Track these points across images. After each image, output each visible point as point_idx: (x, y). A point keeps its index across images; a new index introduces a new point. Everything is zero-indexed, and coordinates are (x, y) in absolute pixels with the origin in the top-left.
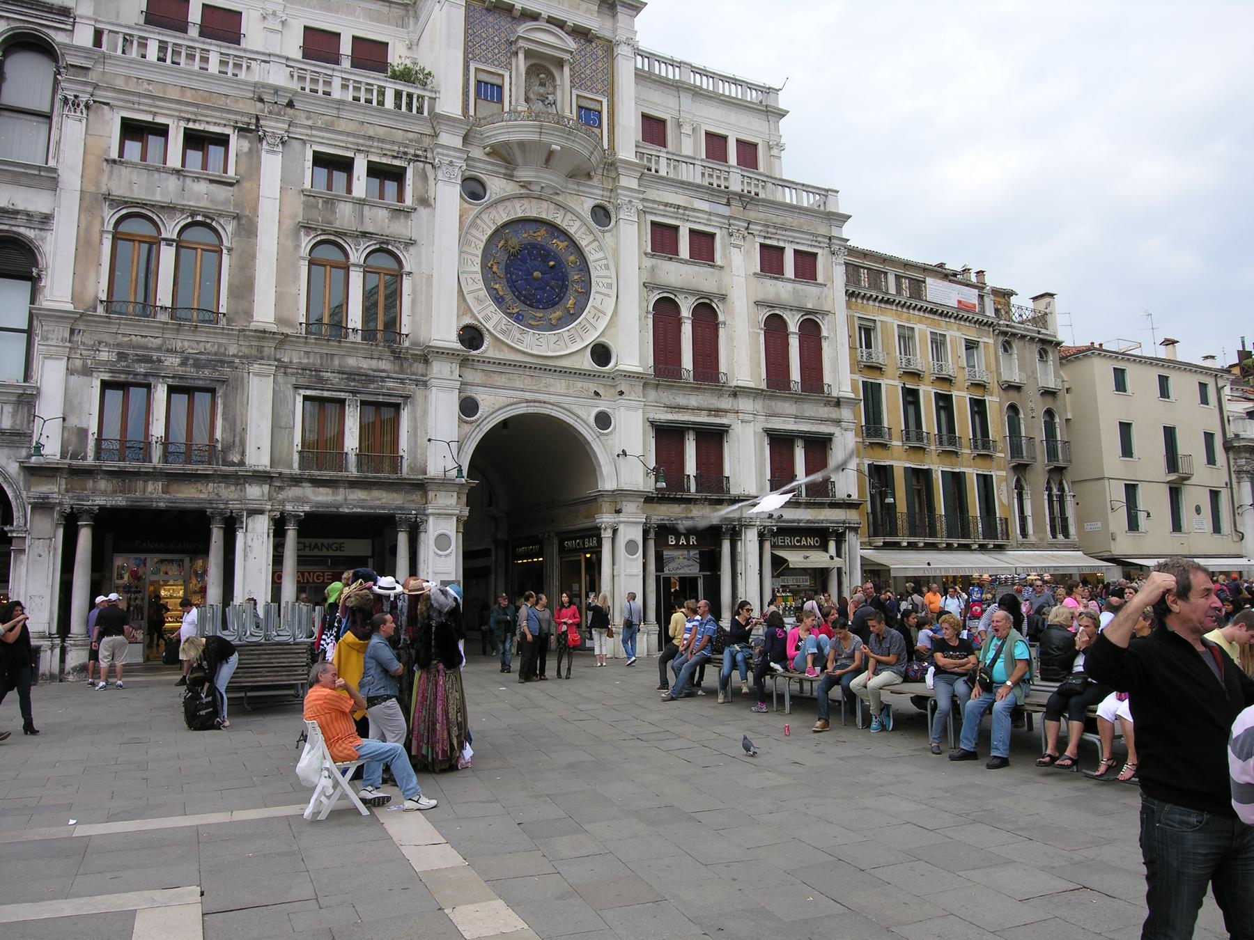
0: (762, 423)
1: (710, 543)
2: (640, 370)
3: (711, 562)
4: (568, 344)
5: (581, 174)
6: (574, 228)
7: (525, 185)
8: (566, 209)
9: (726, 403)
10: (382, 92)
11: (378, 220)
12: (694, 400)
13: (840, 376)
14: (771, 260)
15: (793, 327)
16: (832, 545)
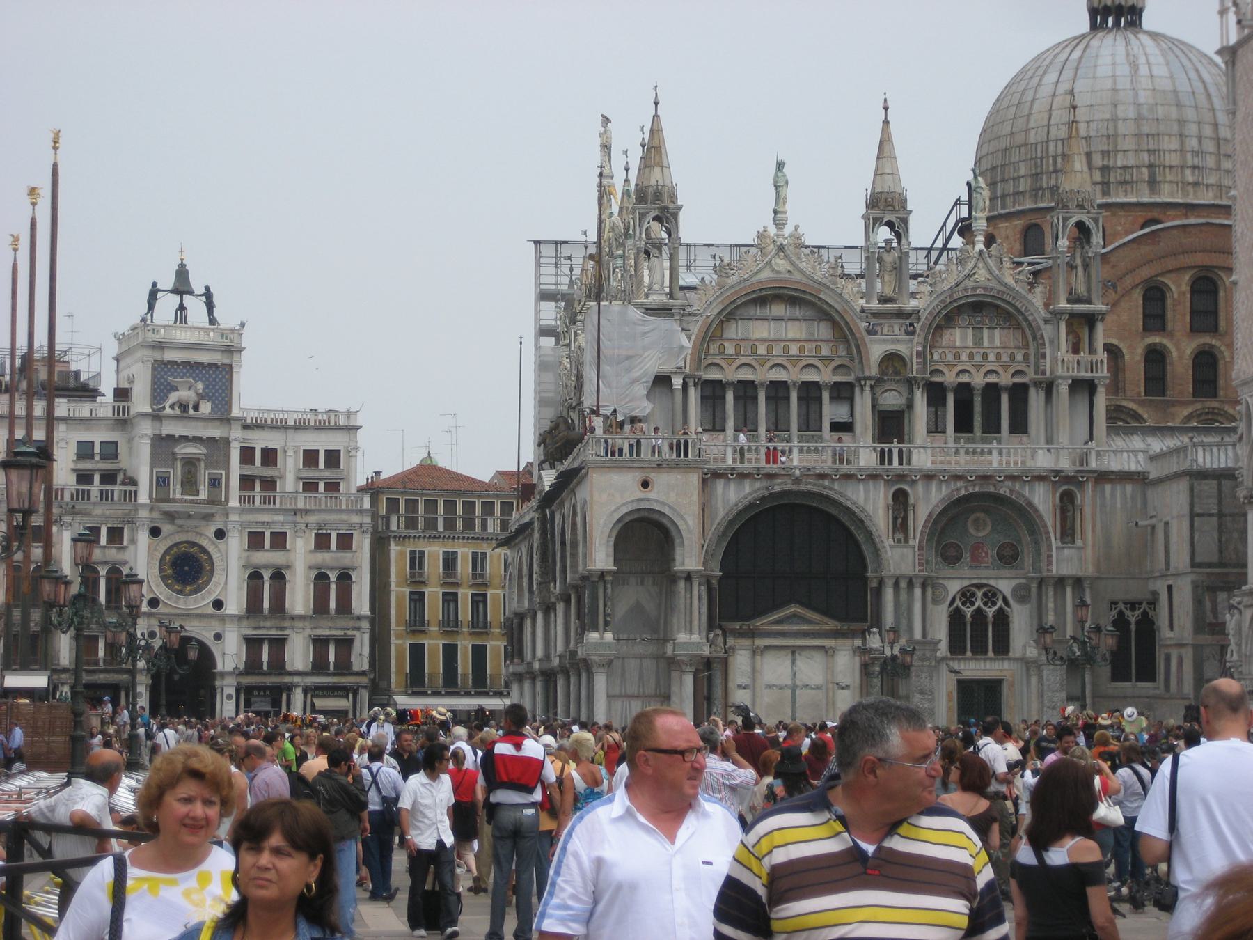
0: (308, 631)
1: (277, 694)
2: (236, 612)
3: (276, 703)
4: (201, 602)
5: (208, 517)
6: (205, 543)
7: (181, 526)
8: (201, 535)
9: (287, 624)
10: (112, 492)
11: (112, 554)
12: (268, 624)
13: (361, 602)
14: (322, 542)
15: (333, 578)
16: (351, 696)
